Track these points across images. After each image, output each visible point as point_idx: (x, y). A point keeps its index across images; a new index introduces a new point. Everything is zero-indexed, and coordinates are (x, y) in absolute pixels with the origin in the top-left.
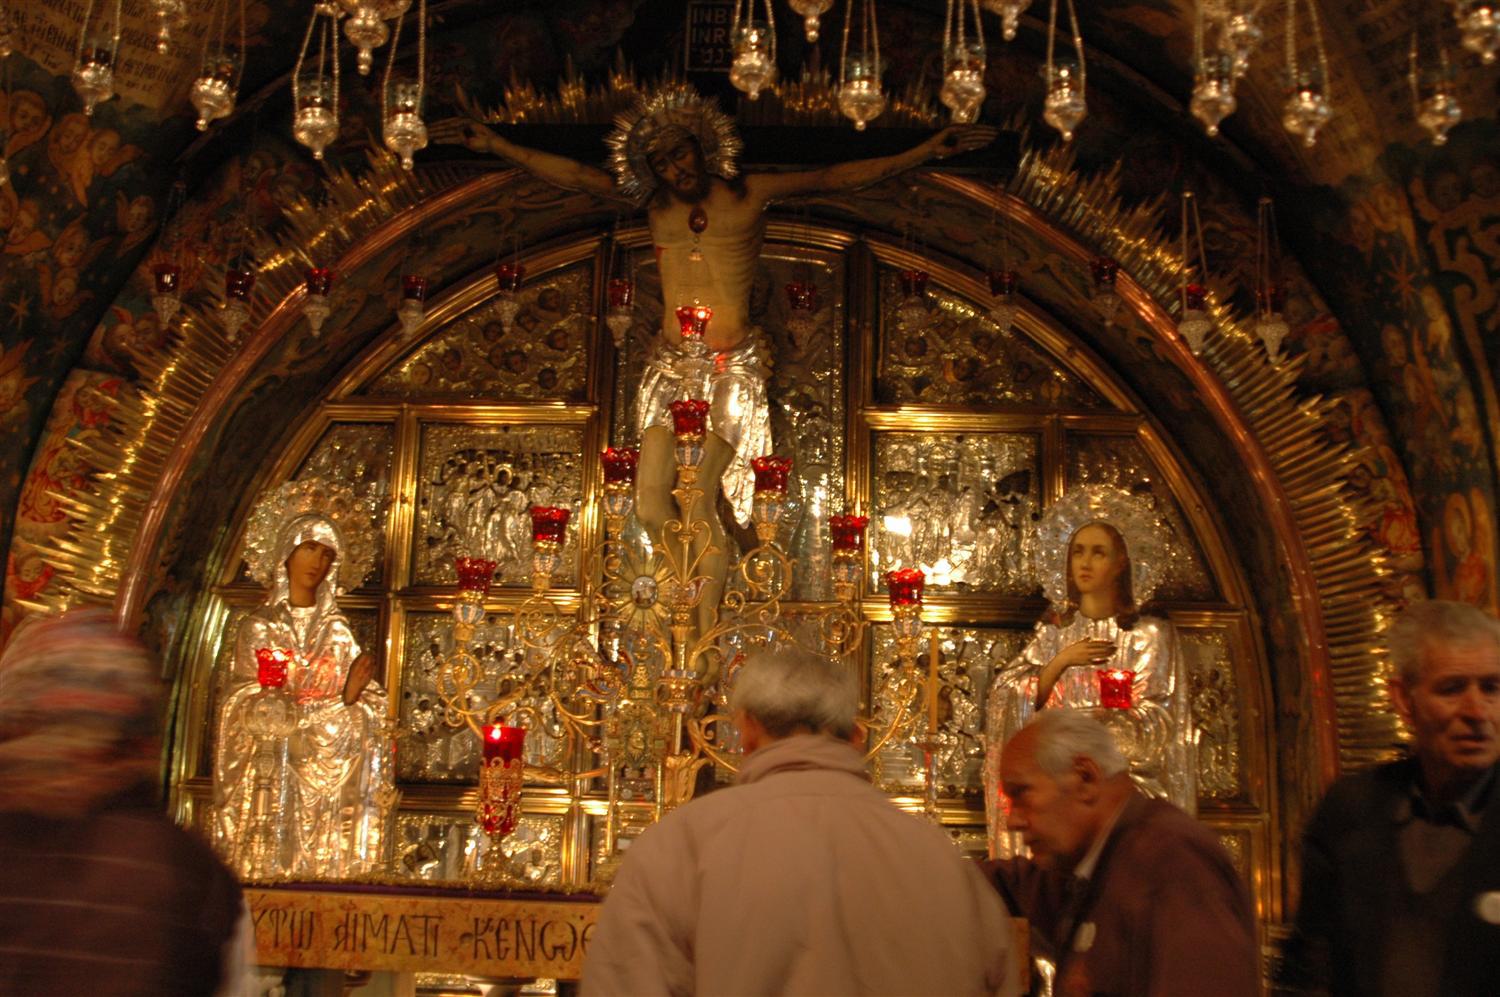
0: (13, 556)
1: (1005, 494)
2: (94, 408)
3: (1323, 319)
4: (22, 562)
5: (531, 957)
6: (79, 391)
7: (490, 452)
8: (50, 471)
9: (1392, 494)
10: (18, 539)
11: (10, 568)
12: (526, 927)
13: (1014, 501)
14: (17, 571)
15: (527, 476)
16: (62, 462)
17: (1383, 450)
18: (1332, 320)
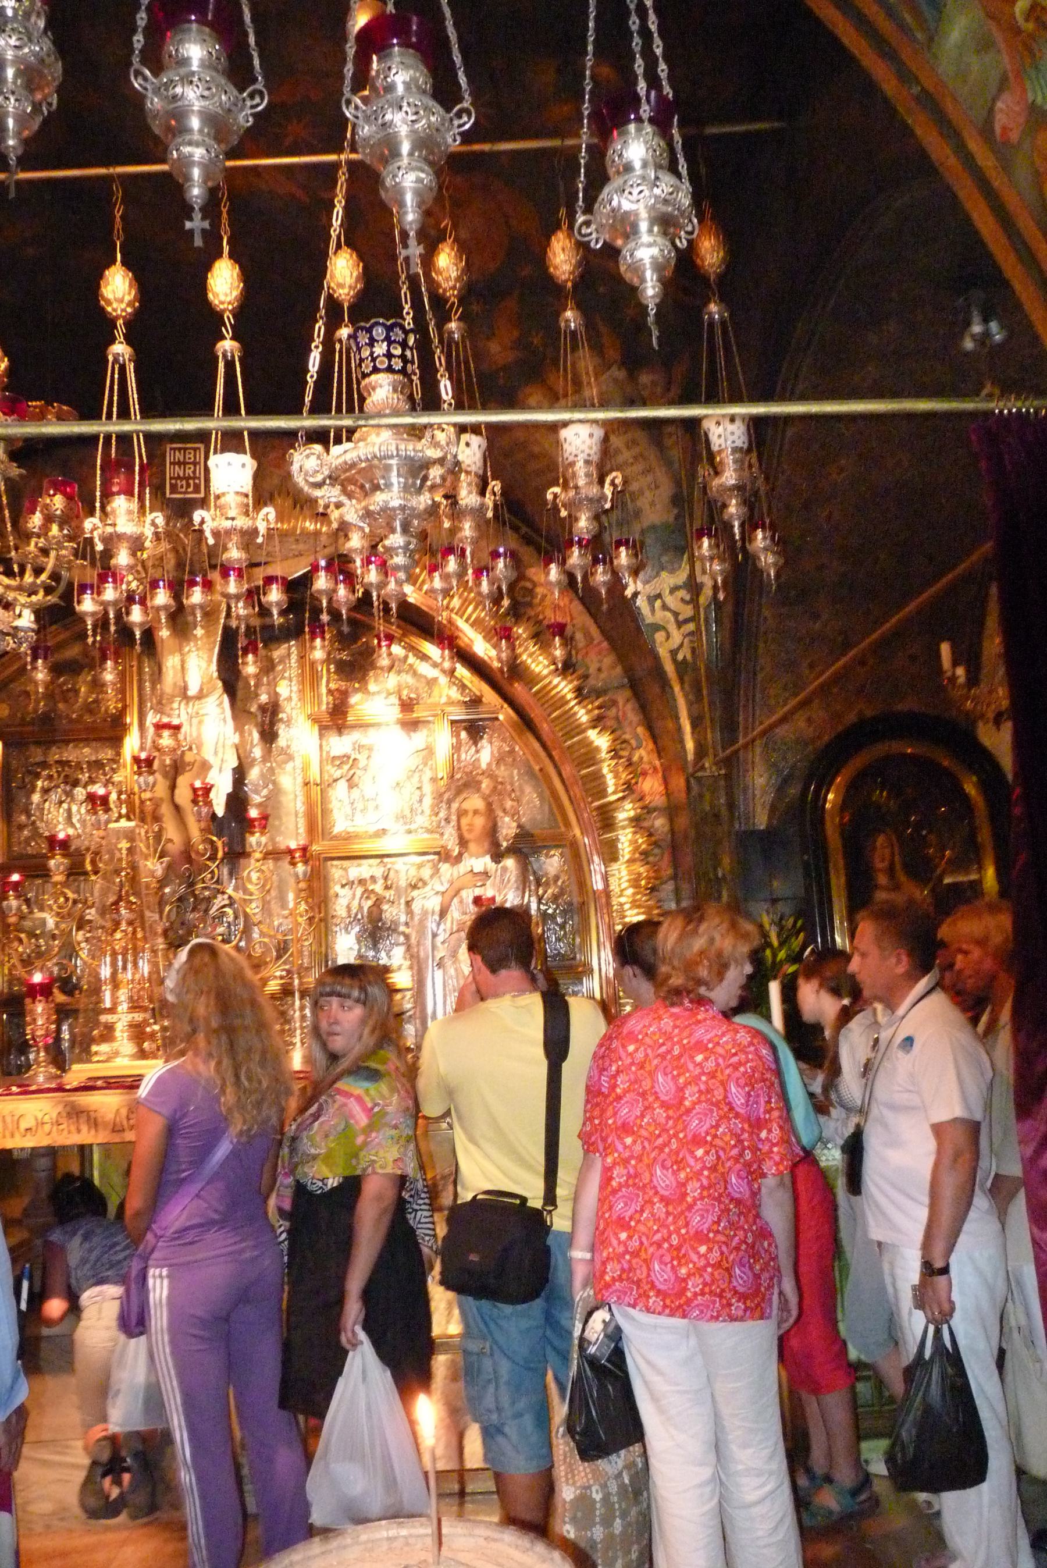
3: (599, 644)
5: (12, 1136)
7: (57, 762)
12: (9, 1119)
15: (84, 777)
17: (640, 730)
18: (605, 644)
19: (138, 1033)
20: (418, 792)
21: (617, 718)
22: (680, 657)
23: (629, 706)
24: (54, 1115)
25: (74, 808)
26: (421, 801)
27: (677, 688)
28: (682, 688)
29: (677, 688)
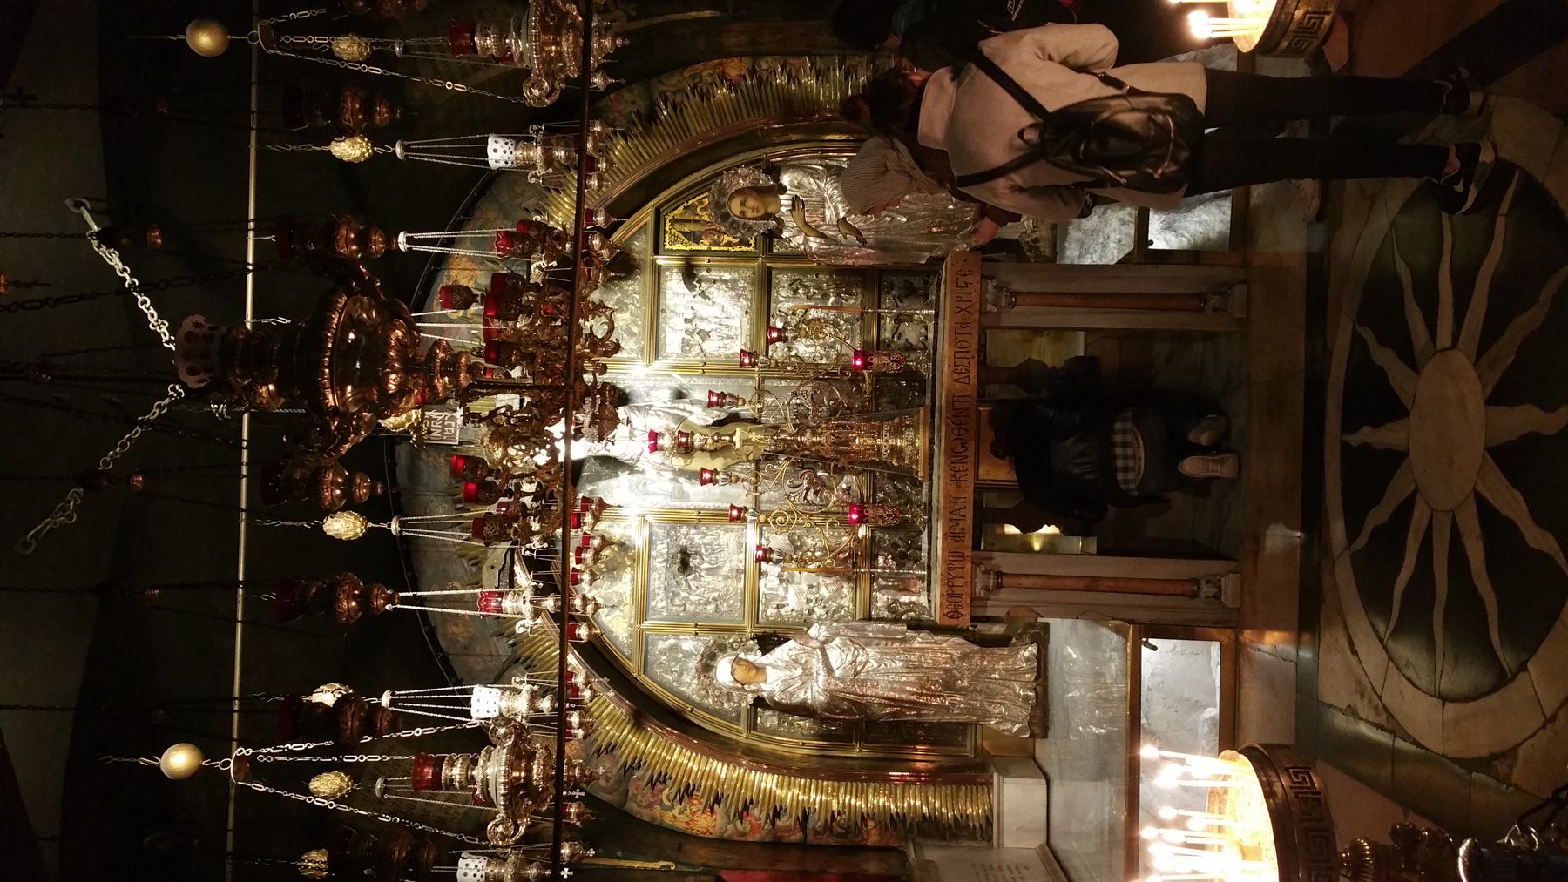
0: (735, 838)
1: (695, 286)
2: (649, 795)
4: (739, 831)
6: (639, 806)
8: (687, 819)
10: (726, 835)
11: (742, 839)
12: (954, 459)
13: (700, 281)
14: (744, 834)
17: (686, 74)
19: (897, 432)
21: (674, 93)
22: (634, 14)
24: (954, 426)
25: (705, 566)
26: (725, 282)
27: (660, 19)
28: (661, 15)
29: (660, 19)
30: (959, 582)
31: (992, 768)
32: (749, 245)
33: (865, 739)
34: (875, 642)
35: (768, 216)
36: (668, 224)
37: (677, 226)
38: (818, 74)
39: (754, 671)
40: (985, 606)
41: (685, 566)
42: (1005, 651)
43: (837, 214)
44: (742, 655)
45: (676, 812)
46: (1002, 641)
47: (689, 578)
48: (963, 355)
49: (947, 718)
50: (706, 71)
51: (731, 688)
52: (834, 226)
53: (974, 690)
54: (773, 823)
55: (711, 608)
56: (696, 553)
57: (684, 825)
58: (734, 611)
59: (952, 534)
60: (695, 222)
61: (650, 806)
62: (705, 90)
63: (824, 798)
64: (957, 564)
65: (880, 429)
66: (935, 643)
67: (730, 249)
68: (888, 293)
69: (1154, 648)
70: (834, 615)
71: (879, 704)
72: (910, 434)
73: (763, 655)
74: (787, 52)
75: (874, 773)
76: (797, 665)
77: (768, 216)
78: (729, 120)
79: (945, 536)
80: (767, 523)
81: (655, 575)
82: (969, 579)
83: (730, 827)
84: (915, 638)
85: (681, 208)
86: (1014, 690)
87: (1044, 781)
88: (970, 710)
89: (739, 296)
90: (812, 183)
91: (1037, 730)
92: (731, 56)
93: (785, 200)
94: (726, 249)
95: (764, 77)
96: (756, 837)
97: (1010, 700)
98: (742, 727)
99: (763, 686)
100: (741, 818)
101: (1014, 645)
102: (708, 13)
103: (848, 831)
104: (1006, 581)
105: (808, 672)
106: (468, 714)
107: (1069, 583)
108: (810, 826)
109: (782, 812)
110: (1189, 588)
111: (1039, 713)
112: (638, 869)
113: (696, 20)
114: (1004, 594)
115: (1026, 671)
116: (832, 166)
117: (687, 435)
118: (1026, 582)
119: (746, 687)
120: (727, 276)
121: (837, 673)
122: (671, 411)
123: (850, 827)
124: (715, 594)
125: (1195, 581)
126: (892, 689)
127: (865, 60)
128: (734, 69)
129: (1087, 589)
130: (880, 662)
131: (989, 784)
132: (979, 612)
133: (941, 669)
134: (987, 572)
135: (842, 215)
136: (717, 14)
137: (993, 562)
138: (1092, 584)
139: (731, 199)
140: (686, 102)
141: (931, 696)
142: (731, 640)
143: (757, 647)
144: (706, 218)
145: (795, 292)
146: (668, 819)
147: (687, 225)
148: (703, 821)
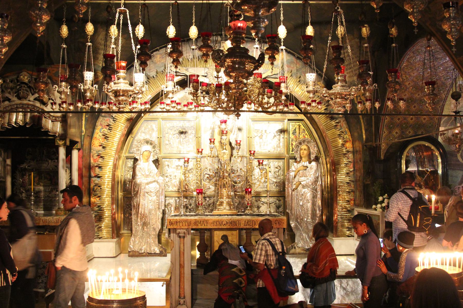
0: (91, 154)
4: (94, 155)
6: (101, 121)
8: (97, 137)
9: (348, 138)
10: (92, 151)
11: (91, 156)
12: (220, 222)
13: (279, 135)
14: (93, 157)
16: (99, 135)
17: (346, 129)
20: (279, 141)
21: (340, 126)
23: (344, 122)
26: (279, 144)
27: (362, 121)
29: (362, 121)
30: (181, 224)
31: (118, 239)
32: (292, 151)
33: (124, 197)
34: (158, 199)
35: (301, 158)
36: (298, 124)
37: (298, 127)
38: (348, 173)
39: (146, 158)
40: (173, 233)
41: (182, 133)
42: (157, 242)
43: (302, 181)
44: (152, 154)
45: (100, 134)
46: (160, 242)
47: (177, 134)
48: (254, 224)
49: (133, 223)
50: (348, 136)
51: (141, 150)
52: (298, 180)
53: (143, 232)
54: (97, 166)
55: (167, 142)
56: (186, 137)
57: (95, 137)
58: (165, 151)
59: (196, 222)
60: (299, 133)
61: (101, 125)
62: (341, 136)
63: (106, 183)
64: (187, 224)
65: (228, 198)
66: (158, 219)
67: (291, 145)
68: (277, 199)
69: (163, 286)
70: (166, 185)
71: (137, 201)
72: (228, 208)
73: (153, 161)
74: (355, 163)
75: (114, 200)
76: (149, 172)
77: (301, 158)
78: (332, 144)
79: (196, 220)
80: (197, 161)
81: (178, 122)
82: (182, 228)
83: (95, 152)
84: (160, 212)
85: (304, 128)
86: (144, 246)
87: (114, 256)
88: (137, 231)
89: (275, 148)
90: (313, 172)
91: (131, 253)
92: (353, 144)
93: (307, 164)
94: (291, 143)
95: (347, 155)
96: (92, 161)
97: (140, 245)
98: (127, 155)
99: (142, 161)
100: (98, 155)
101: (159, 245)
102: (364, 137)
103: (95, 191)
104: (182, 239)
105: (147, 176)
106: (136, 72)
107: (182, 259)
108: (96, 179)
109: (100, 169)
110: (182, 295)
111: (137, 254)
112: (82, 123)
113: (362, 133)
114: (178, 239)
115: (150, 249)
116: (318, 179)
117: (226, 134)
118: (182, 245)
119: (141, 156)
120: (281, 144)
121: (147, 186)
122: (234, 128)
123: (96, 192)
124: (172, 144)
125: (184, 298)
126: (142, 205)
127: (353, 188)
128: (349, 145)
129: (180, 265)
130: (151, 201)
131: (113, 238)
132: (171, 231)
133: (150, 221)
134: (184, 233)
135: (302, 183)
136: (364, 140)
137: (188, 235)
138: (182, 266)
139: (307, 145)
140: (337, 129)
141: (141, 218)
142: (157, 150)
143: (155, 159)
144: (301, 136)
145: (277, 168)
146: (97, 131)
147: (298, 130)
148: (97, 143)
